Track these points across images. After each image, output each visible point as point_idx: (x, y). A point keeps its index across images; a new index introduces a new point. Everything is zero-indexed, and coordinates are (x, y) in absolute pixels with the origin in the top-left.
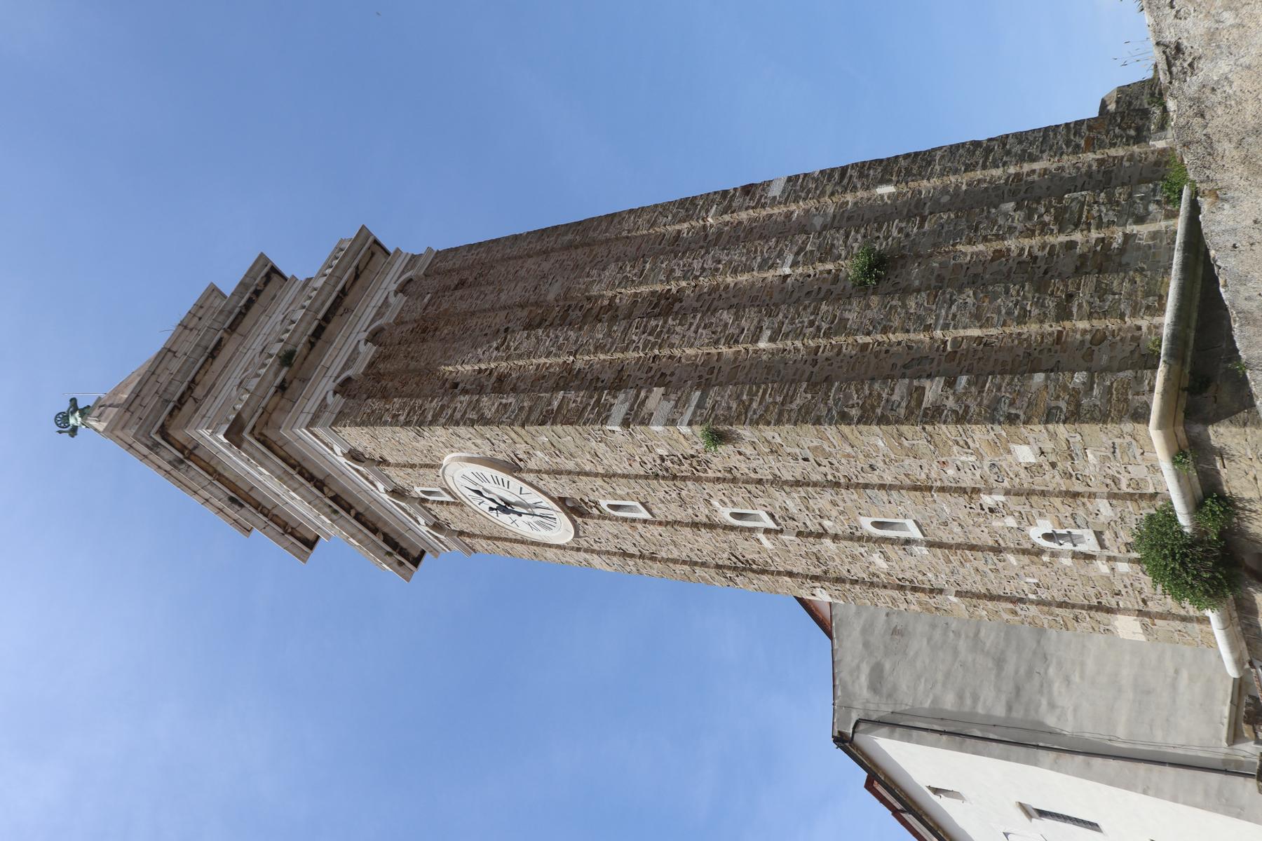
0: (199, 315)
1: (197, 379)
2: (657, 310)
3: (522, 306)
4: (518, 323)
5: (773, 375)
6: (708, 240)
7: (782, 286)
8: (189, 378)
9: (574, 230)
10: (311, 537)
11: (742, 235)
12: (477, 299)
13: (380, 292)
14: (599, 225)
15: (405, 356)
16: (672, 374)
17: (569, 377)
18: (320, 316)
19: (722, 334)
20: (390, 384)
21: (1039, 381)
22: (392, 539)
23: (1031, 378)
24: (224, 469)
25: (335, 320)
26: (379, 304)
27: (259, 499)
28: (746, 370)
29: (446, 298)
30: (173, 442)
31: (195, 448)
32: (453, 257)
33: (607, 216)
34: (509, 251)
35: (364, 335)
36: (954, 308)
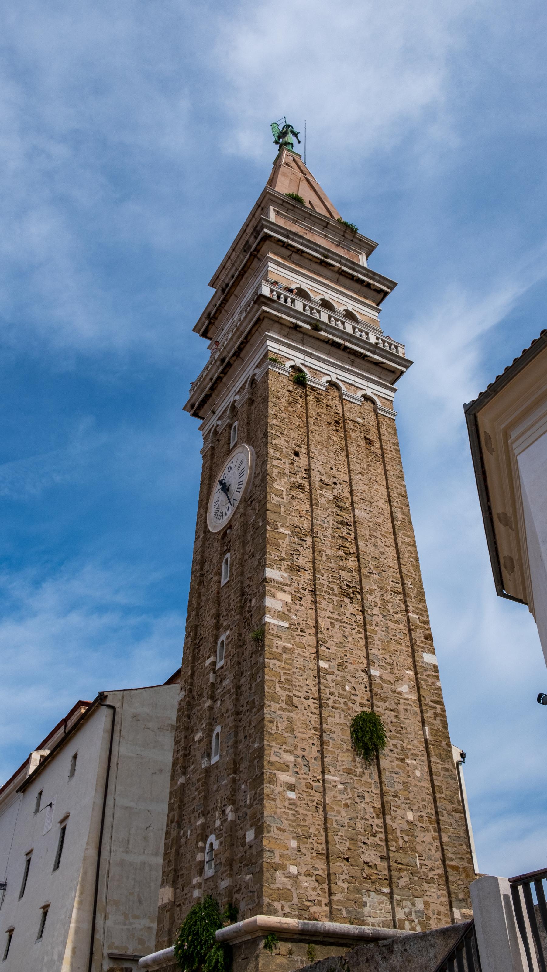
0: (355, 240)
2: (345, 587)
3: (351, 492)
4: (339, 491)
6: (393, 614)
7: (360, 670)
9: (405, 519)
10: (209, 335)
11: (396, 638)
12: (358, 458)
14: (408, 536)
16: (301, 605)
17: (301, 535)
19: (326, 635)
20: (299, 406)
21: (292, 844)
22: (208, 400)
23: (294, 838)
24: (247, 278)
25: (346, 355)
26: (357, 385)
27: (230, 301)
28: (302, 654)
29: (359, 434)
30: (261, 244)
31: (259, 259)
32: (390, 433)
33: (414, 541)
34: (392, 473)
36: (341, 786)
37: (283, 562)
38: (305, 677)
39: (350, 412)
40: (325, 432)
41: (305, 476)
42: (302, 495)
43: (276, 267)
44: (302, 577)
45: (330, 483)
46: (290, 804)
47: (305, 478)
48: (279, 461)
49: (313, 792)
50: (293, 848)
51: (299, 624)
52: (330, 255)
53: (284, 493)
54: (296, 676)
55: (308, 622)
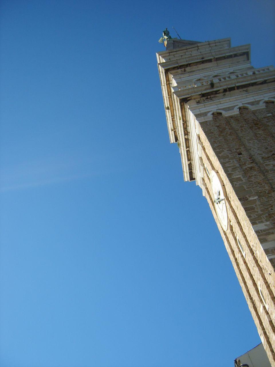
1: (191, 65)
8: (190, 62)
13: (262, 96)
15: (241, 126)
18: (237, 85)
30: (167, 76)
35: (240, 105)
39: (260, 114)
40: (251, 132)
41: (252, 161)
42: (255, 173)
45: (269, 155)
47: (252, 163)
53: (242, 178)
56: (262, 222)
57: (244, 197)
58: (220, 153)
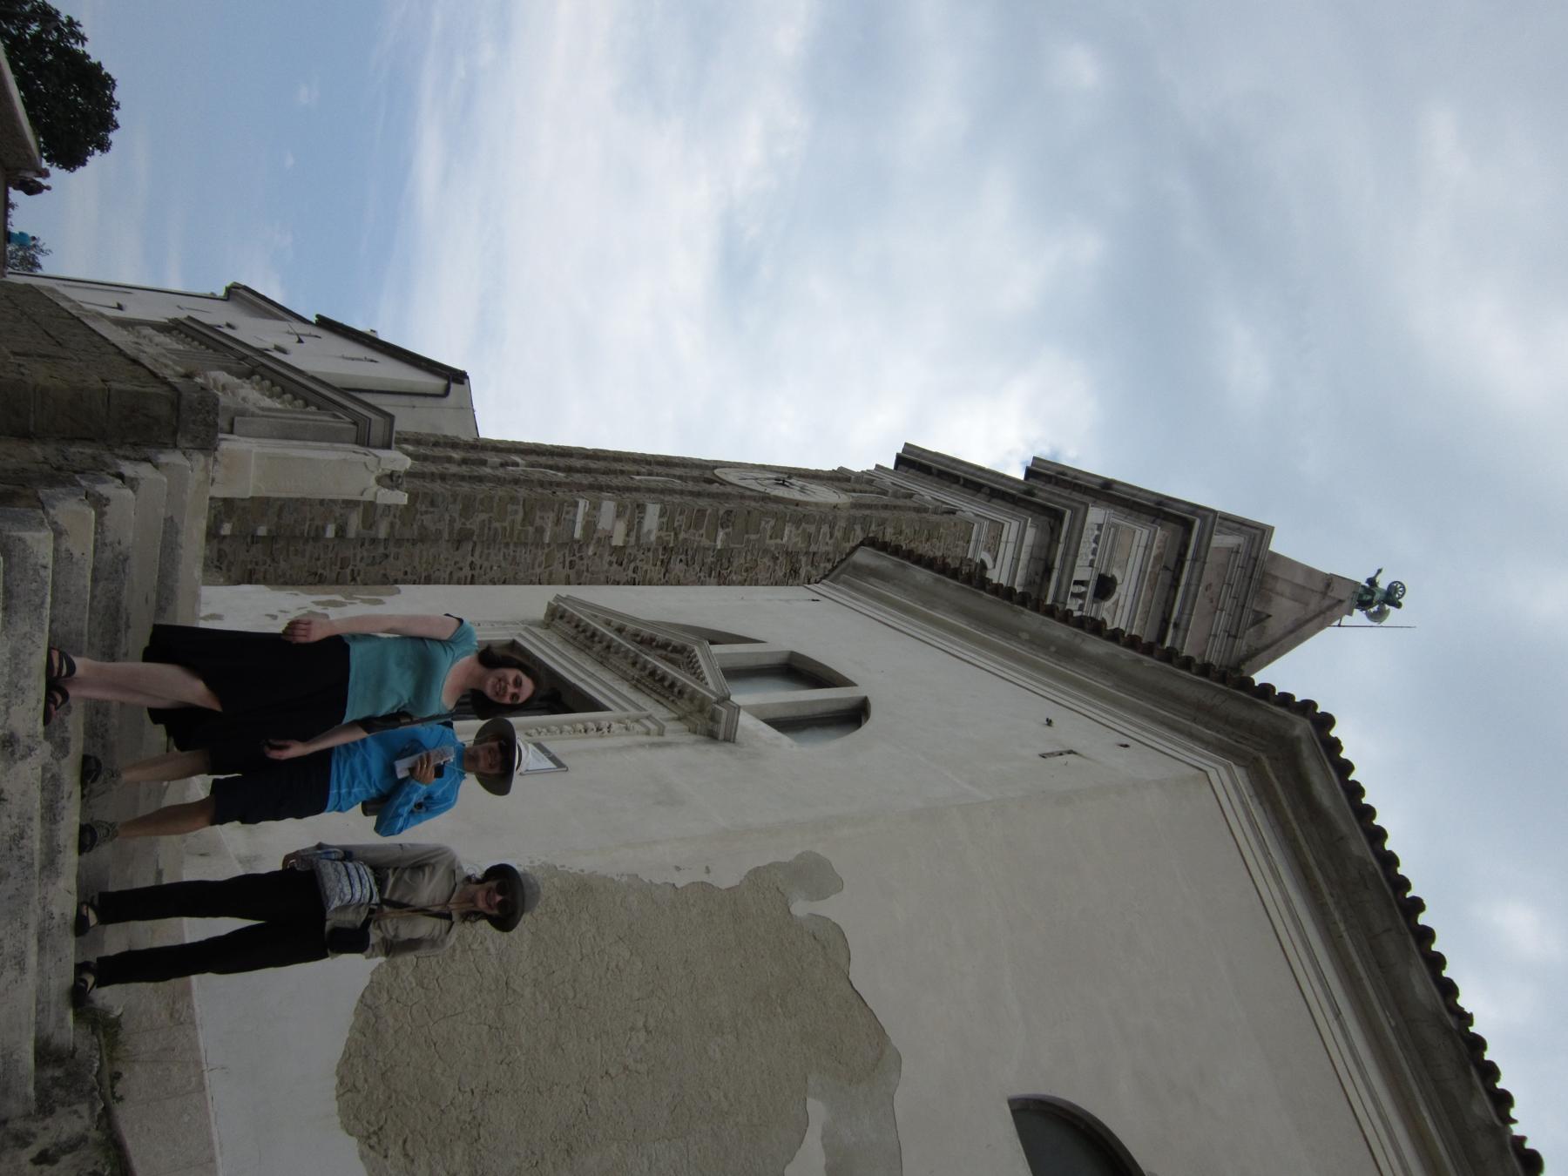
5: (509, 555)
21: (262, 528)
23: (269, 531)
37: (672, 534)
38: (503, 565)
42: (781, 574)
43: (1143, 543)
44: (653, 568)
46: (317, 527)
48: (828, 536)
49: (337, 568)
50: (255, 530)
51: (581, 558)
52: (1181, 634)
53: (779, 541)
54: (503, 550)
55: (585, 574)
56: (661, 529)
57: (730, 524)
58: (862, 528)
